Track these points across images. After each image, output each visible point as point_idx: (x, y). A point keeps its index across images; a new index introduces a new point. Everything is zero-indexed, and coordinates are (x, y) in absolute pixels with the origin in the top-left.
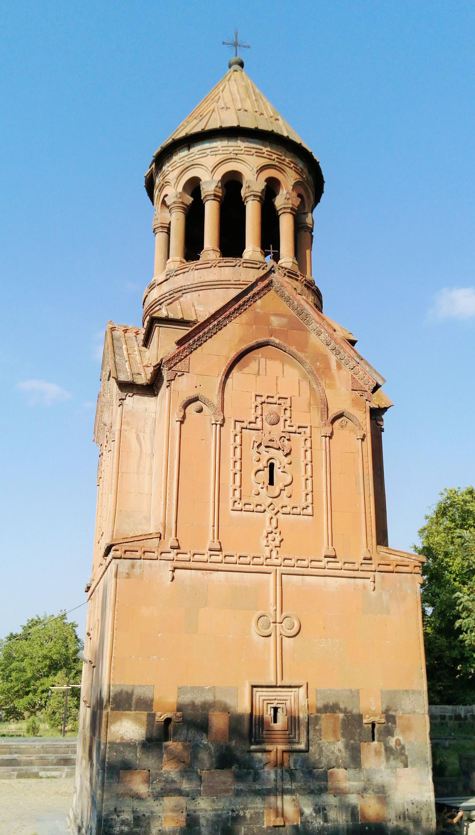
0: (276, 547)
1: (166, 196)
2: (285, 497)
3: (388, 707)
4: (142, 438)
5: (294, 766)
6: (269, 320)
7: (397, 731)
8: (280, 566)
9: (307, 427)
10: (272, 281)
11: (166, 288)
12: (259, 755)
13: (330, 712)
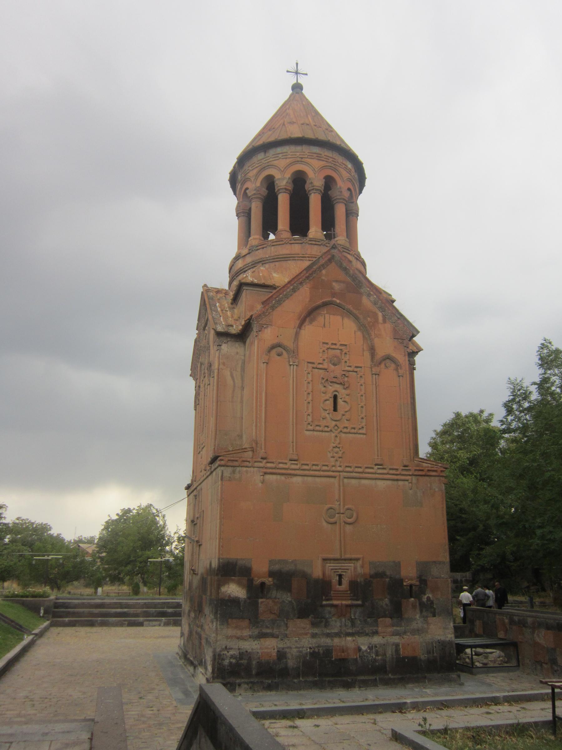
0: (339, 458)
1: (247, 189)
2: (346, 421)
4: (234, 375)
7: (428, 591)
11: (249, 259)
12: (329, 609)
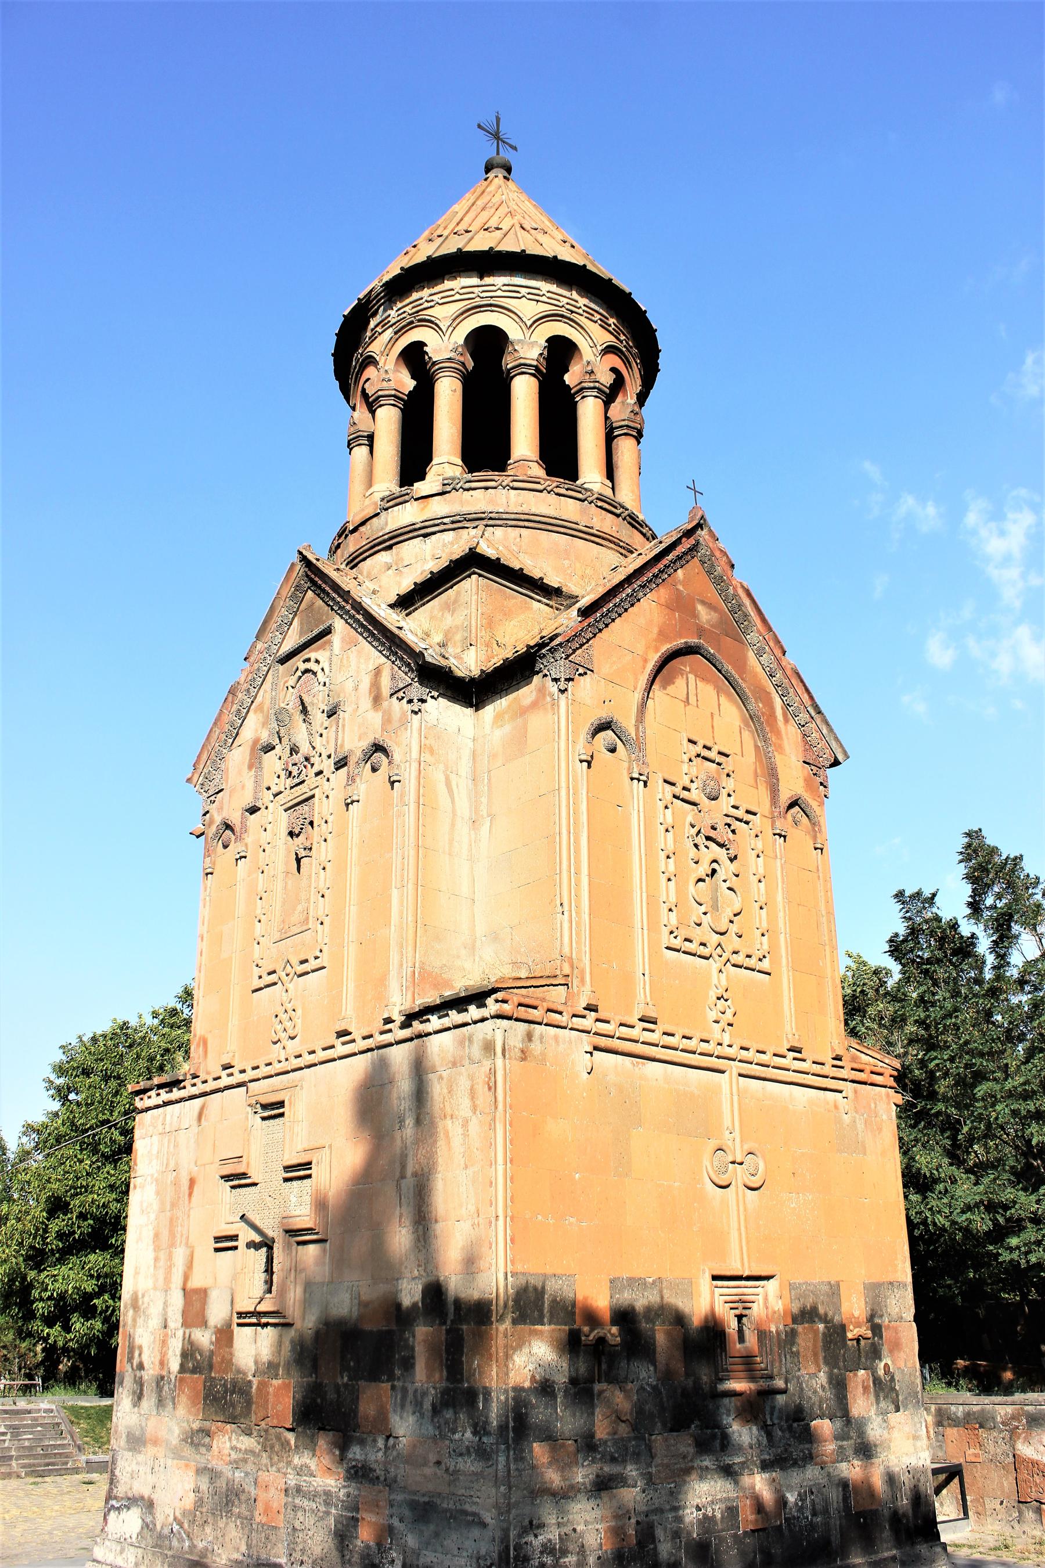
3: (872, 1310)
4: (454, 787)
5: (771, 1419)
6: (694, 609)
7: (885, 1351)
8: (734, 1060)
9: (755, 814)
10: (698, 543)
11: (439, 508)
13: (807, 1322)
